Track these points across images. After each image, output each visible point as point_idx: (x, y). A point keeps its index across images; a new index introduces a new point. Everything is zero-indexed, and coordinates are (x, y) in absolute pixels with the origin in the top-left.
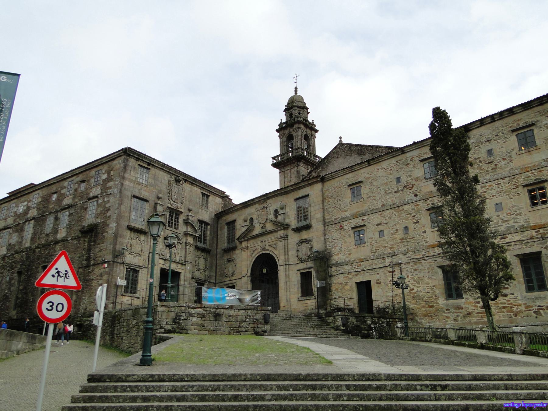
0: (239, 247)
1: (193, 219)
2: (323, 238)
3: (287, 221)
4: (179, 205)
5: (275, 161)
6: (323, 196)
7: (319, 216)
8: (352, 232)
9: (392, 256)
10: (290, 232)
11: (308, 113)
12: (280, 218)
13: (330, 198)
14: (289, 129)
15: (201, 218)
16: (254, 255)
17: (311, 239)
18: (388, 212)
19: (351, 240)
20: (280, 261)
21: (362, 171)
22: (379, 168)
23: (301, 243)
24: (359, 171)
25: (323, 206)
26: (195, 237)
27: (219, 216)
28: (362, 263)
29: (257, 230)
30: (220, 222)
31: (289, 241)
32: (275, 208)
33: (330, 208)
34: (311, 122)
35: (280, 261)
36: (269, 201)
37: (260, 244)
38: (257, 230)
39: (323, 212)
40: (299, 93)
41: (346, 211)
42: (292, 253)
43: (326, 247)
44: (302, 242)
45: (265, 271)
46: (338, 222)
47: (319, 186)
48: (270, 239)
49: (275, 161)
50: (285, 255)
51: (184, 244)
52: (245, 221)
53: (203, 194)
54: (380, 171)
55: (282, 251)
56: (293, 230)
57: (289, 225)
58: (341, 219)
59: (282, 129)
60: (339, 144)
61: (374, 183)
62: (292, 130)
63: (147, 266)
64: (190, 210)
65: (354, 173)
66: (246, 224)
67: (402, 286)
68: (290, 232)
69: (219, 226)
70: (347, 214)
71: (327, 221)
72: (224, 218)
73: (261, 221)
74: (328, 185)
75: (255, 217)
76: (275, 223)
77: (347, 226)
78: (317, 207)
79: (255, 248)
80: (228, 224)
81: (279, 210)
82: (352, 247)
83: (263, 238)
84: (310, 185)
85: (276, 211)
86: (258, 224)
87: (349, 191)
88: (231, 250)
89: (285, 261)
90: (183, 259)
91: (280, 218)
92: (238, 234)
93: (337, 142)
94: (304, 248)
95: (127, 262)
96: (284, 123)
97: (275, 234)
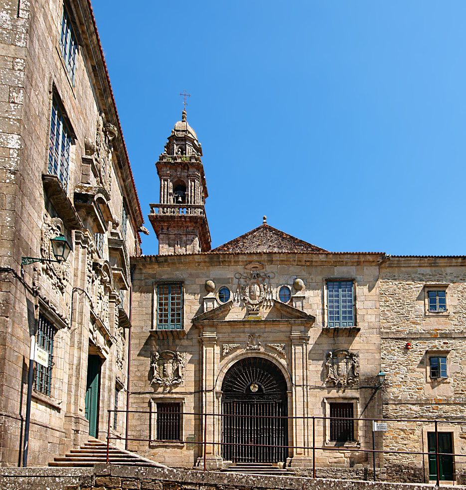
41: (418, 324)
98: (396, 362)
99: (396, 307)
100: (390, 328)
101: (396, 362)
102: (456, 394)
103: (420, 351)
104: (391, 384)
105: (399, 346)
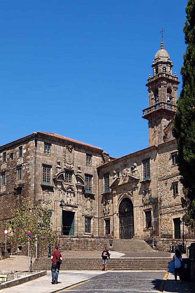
4: (72, 166)
5: (146, 113)
15: (87, 172)
46: (165, 178)
53: (87, 155)
64: (79, 168)
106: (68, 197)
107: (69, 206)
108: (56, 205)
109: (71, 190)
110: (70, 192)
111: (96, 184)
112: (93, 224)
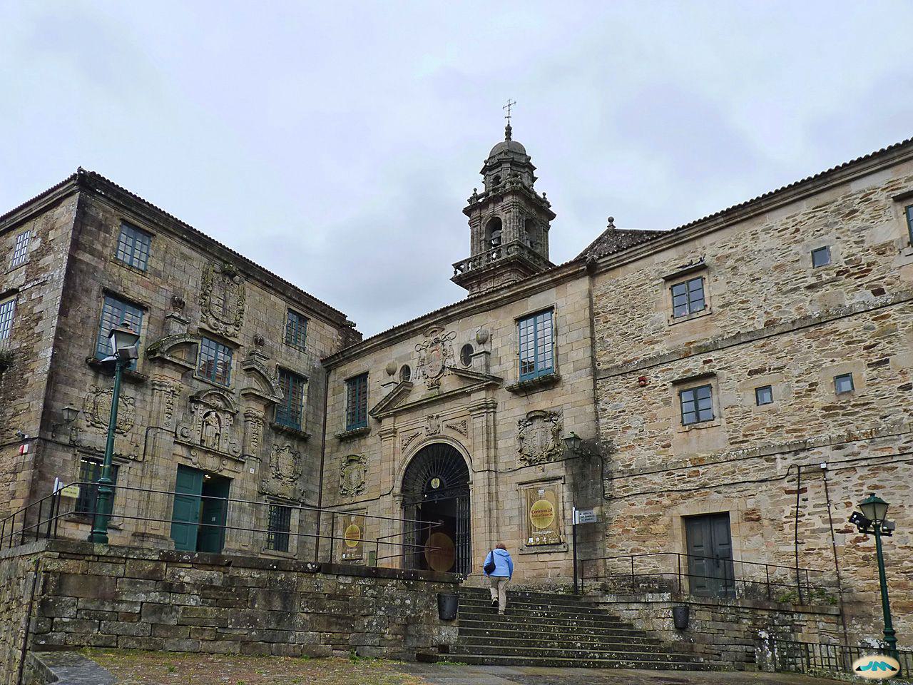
0: (375, 430)
1: (268, 365)
2: (590, 408)
3: (495, 370)
6: (591, 308)
7: (582, 355)
8: (673, 392)
9: (797, 452)
10: (502, 396)
11: (534, 179)
12: (477, 364)
13: (613, 312)
14: (491, 206)
15: (286, 364)
16: (410, 447)
17: (556, 410)
18: (785, 338)
19: (668, 411)
20: (476, 460)
21: (707, 240)
22: (759, 229)
23: (532, 419)
24: (697, 242)
25: (592, 332)
26: (270, 405)
27: (330, 364)
28: (701, 470)
29: (420, 391)
30: (332, 378)
31: (499, 416)
32: (464, 341)
33: (609, 336)
34: (542, 197)
35: (476, 462)
36: (449, 328)
37: (425, 424)
38: (420, 391)
39: (593, 346)
40: (514, 138)
42: (507, 444)
43: (598, 429)
44: (531, 418)
45: (436, 483)
46: (631, 368)
47: (583, 284)
48: (450, 411)
49: (459, 272)
50: (488, 448)
51: (241, 418)
52: (391, 373)
54: (762, 236)
55: (481, 439)
56: (511, 389)
57: (501, 380)
58: (645, 361)
59: (474, 208)
60: (607, 232)
61: (743, 269)
62: (498, 208)
63: (140, 458)
65: (681, 248)
66: (391, 379)
67: (876, 527)
68: (502, 396)
69: (331, 385)
70: (661, 349)
71: (603, 367)
72: (342, 369)
73: (428, 373)
74: (604, 283)
75: (413, 365)
76: (462, 375)
77: (657, 377)
78: (574, 335)
79: (413, 433)
80: (351, 381)
81: (474, 344)
82: (674, 429)
83: (434, 411)
84: (557, 283)
85: (467, 349)
86: (422, 380)
87: (666, 293)
88: (355, 434)
89: (488, 462)
90: (238, 448)
91: (477, 364)
92: (373, 402)
93: (603, 228)
94: (539, 436)
95: (85, 443)
96: (482, 196)
97: (465, 400)
98: (624, 411)
99: (621, 327)
100: (612, 361)
101: (624, 411)
102: (732, 444)
103: (664, 385)
104: (619, 447)
105: (628, 385)
106: (208, 424)
107: (207, 452)
108: (150, 441)
109: (220, 404)
110: (217, 409)
111: (316, 408)
112: (297, 523)
